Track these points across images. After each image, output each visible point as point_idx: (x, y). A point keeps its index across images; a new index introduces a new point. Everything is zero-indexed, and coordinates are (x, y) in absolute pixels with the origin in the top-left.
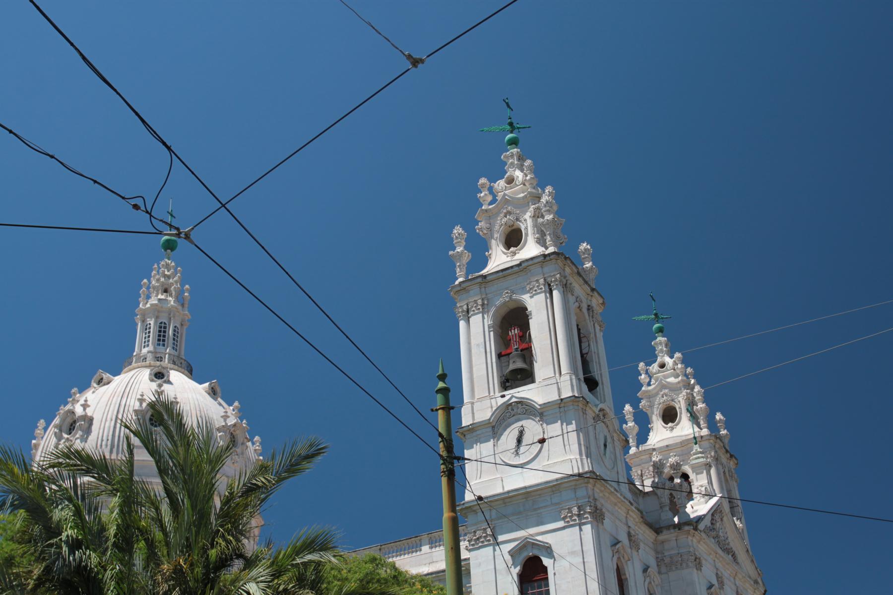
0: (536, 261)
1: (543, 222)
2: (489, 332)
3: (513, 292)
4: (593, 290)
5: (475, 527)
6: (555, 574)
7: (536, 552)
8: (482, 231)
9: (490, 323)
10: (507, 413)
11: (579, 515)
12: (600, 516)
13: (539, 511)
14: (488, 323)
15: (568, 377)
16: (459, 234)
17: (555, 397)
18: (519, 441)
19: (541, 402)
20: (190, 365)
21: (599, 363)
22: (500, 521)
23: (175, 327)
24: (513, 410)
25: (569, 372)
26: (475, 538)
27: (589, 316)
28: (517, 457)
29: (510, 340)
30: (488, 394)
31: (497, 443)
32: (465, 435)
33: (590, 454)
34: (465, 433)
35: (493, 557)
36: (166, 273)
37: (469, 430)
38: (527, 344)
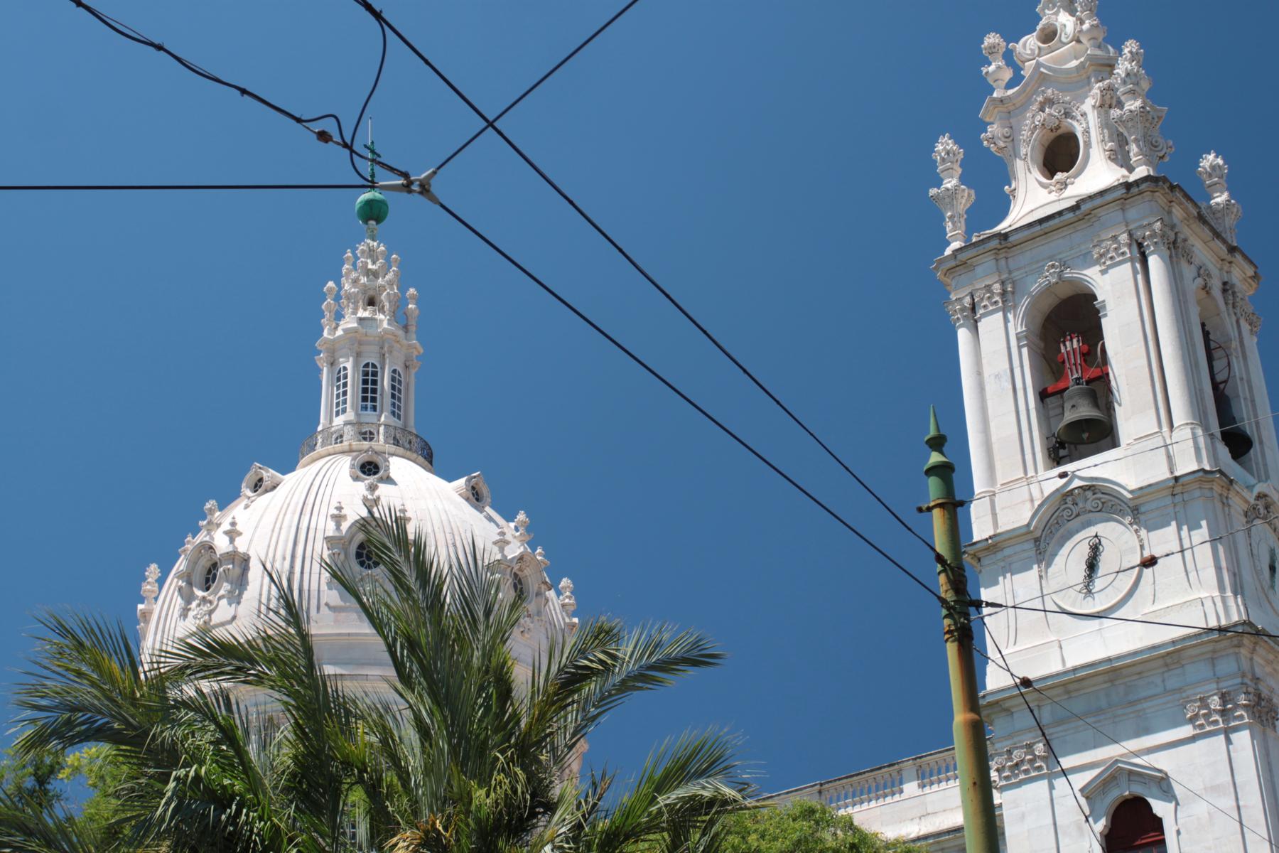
0: (1109, 197)
1: (1121, 116)
2: (1020, 348)
3: (1065, 265)
4: (1232, 250)
5: (1009, 742)
6: (1178, 832)
7: (1138, 790)
8: (995, 143)
9: (1019, 330)
10: (1064, 510)
11: (1223, 713)
12: (1268, 712)
13: (1139, 707)
14: (1016, 329)
15: (1187, 433)
16: (948, 153)
17: (1162, 474)
18: (1092, 566)
19: (1133, 485)
20: (427, 444)
21: (1253, 401)
22: (1060, 728)
23: (394, 371)
24: (1077, 504)
25: (1189, 422)
26: (1009, 764)
27: (1226, 304)
28: (1089, 599)
29: (1064, 362)
30: (1022, 475)
31: (1047, 572)
32: (979, 560)
33: (1242, 588)
34: (980, 555)
35: (1048, 800)
36: (370, 266)
37: (987, 549)
38: (1099, 369)
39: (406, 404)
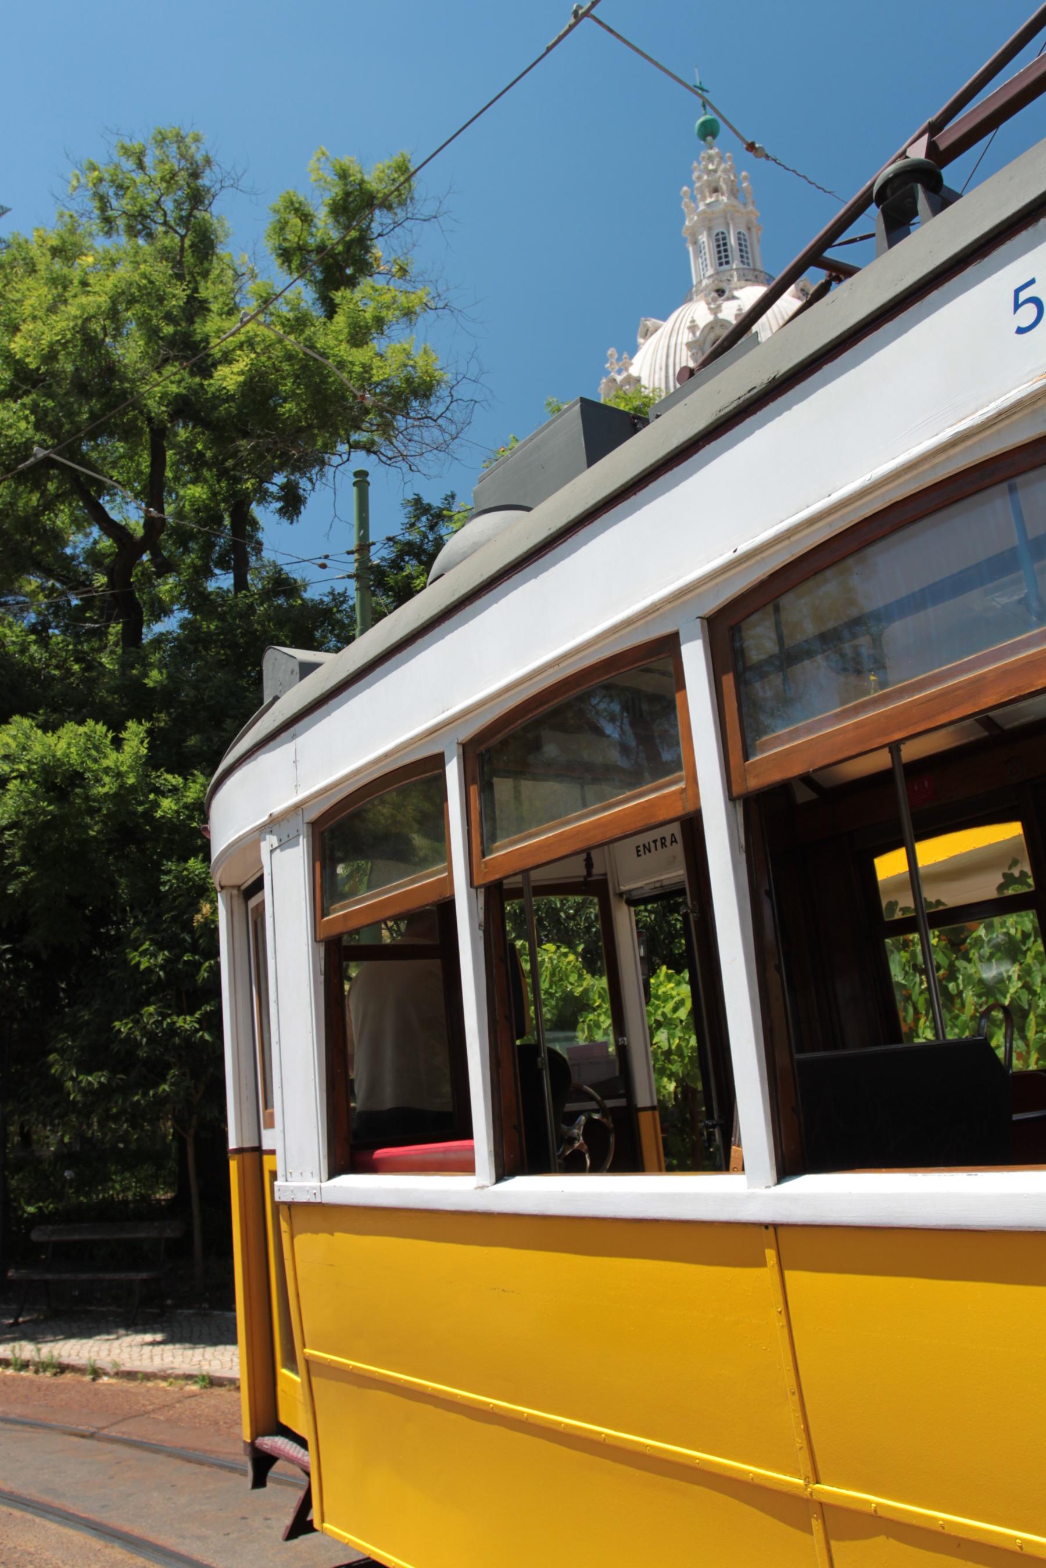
23: (739, 233)
36: (711, 167)
39: (753, 254)
